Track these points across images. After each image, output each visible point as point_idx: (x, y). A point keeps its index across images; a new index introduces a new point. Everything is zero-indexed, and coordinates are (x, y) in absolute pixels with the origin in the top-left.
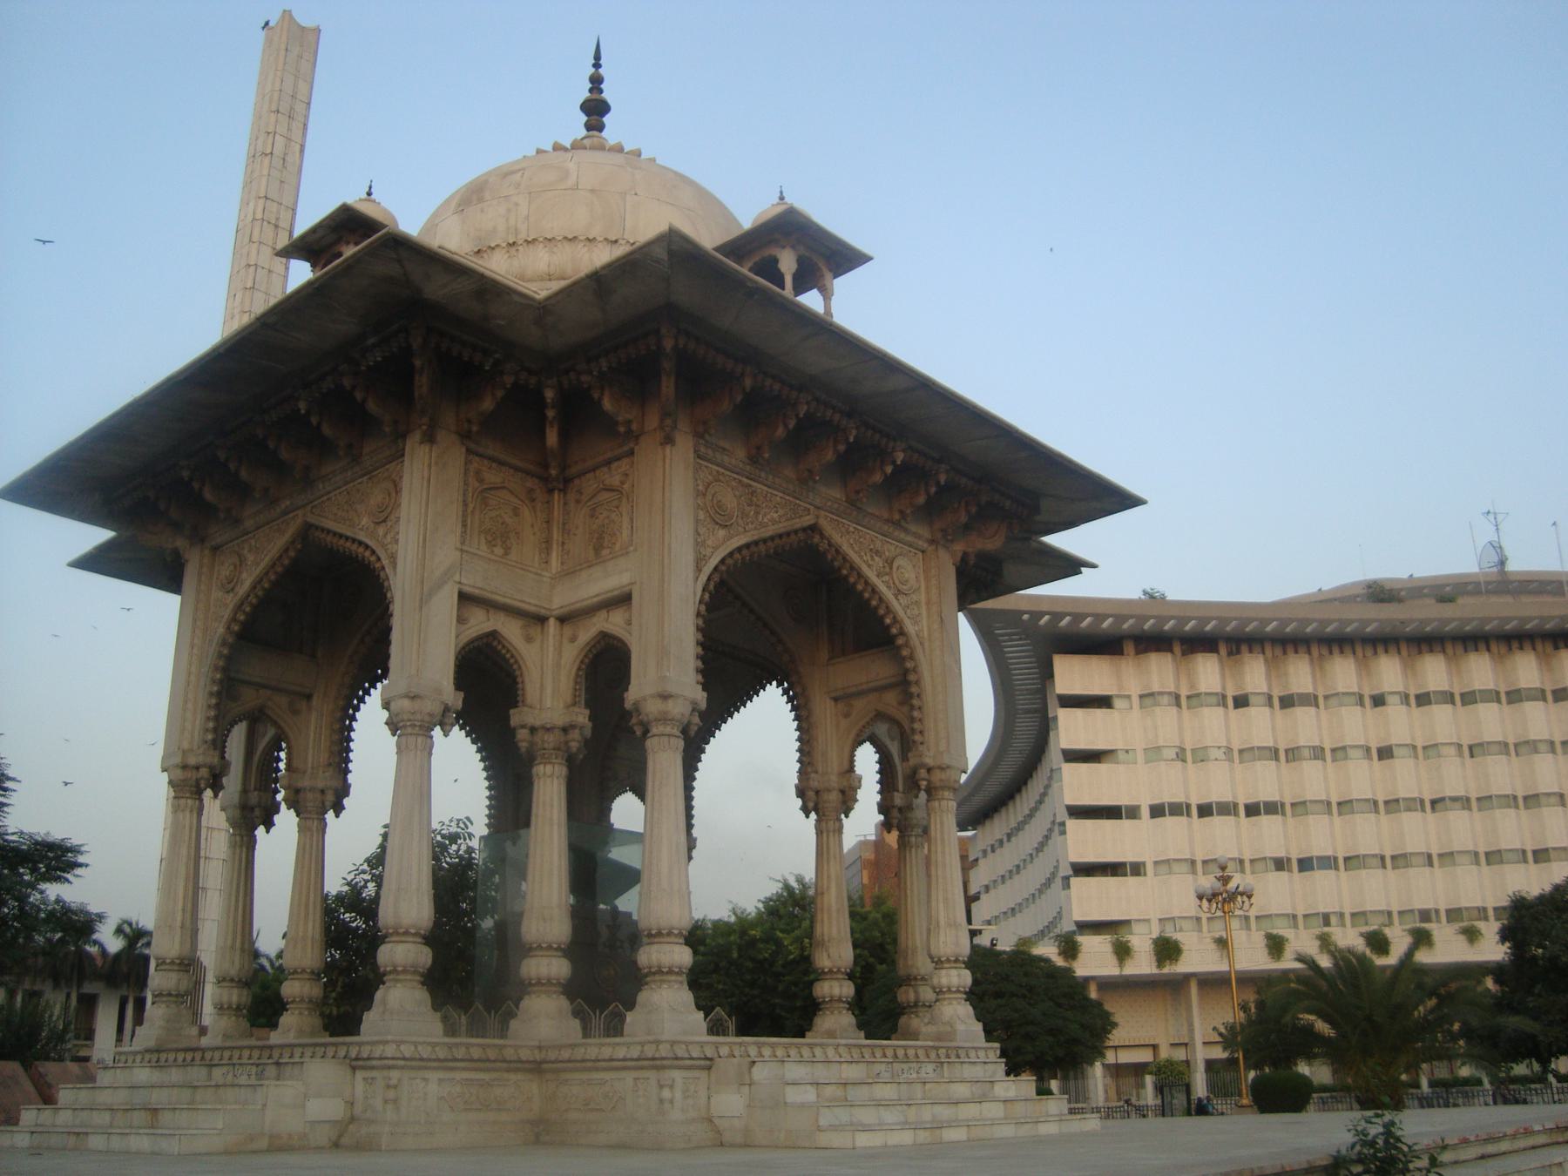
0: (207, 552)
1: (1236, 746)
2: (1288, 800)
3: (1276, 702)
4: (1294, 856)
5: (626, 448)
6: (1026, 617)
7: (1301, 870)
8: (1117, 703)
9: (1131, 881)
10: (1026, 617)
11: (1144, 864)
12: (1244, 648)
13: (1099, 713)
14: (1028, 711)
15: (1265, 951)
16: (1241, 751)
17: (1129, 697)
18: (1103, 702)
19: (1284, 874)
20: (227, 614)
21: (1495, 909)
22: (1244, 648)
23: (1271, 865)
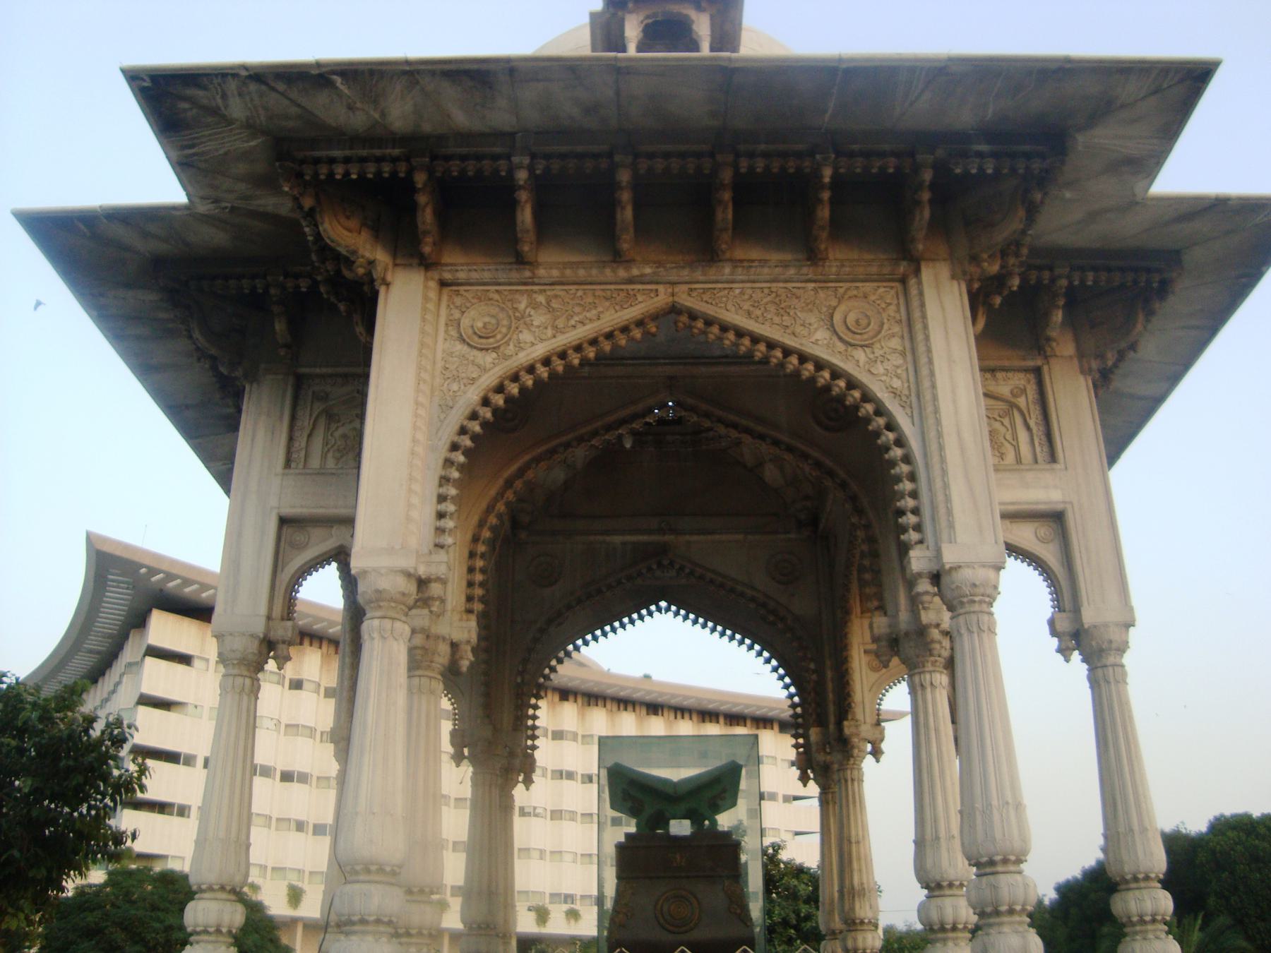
0: (433, 284)
1: (284, 721)
2: (316, 774)
3: (322, 690)
4: (312, 821)
5: (1030, 363)
6: (143, 570)
7: (315, 833)
8: (196, 663)
9: (175, 820)
10: (143, 570)
11: (190, 807)
12: (306, 642)
13: (180, 668)
14: (91, 651)
15: (286, 899)
16: (287, 726)
17: (207, 660)
18: (185, 659)
19: (301, 835)
20: (489, 380)
21: (452, 887)
22: (306, 642)
23: (293, 825)
